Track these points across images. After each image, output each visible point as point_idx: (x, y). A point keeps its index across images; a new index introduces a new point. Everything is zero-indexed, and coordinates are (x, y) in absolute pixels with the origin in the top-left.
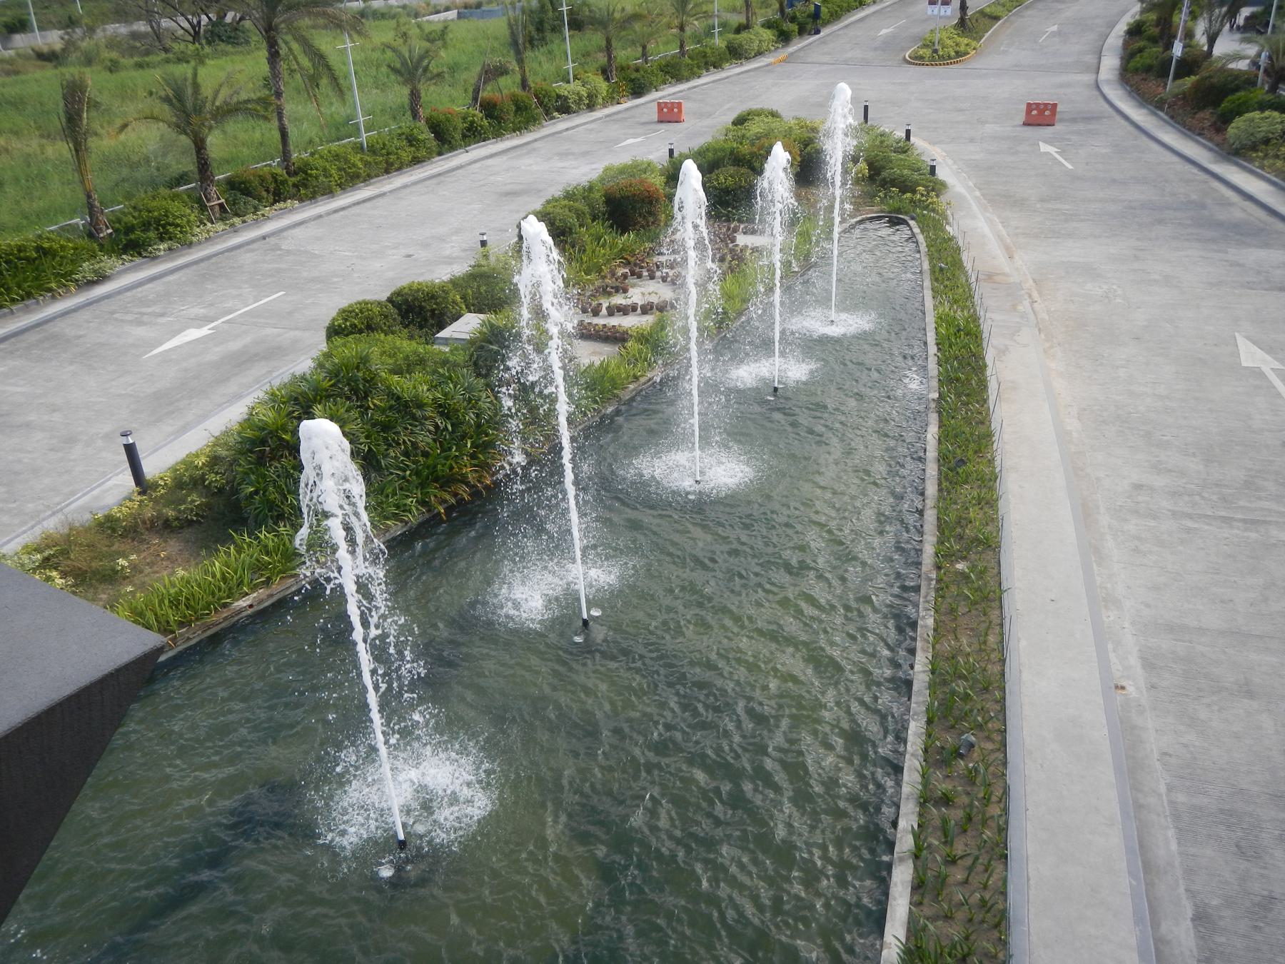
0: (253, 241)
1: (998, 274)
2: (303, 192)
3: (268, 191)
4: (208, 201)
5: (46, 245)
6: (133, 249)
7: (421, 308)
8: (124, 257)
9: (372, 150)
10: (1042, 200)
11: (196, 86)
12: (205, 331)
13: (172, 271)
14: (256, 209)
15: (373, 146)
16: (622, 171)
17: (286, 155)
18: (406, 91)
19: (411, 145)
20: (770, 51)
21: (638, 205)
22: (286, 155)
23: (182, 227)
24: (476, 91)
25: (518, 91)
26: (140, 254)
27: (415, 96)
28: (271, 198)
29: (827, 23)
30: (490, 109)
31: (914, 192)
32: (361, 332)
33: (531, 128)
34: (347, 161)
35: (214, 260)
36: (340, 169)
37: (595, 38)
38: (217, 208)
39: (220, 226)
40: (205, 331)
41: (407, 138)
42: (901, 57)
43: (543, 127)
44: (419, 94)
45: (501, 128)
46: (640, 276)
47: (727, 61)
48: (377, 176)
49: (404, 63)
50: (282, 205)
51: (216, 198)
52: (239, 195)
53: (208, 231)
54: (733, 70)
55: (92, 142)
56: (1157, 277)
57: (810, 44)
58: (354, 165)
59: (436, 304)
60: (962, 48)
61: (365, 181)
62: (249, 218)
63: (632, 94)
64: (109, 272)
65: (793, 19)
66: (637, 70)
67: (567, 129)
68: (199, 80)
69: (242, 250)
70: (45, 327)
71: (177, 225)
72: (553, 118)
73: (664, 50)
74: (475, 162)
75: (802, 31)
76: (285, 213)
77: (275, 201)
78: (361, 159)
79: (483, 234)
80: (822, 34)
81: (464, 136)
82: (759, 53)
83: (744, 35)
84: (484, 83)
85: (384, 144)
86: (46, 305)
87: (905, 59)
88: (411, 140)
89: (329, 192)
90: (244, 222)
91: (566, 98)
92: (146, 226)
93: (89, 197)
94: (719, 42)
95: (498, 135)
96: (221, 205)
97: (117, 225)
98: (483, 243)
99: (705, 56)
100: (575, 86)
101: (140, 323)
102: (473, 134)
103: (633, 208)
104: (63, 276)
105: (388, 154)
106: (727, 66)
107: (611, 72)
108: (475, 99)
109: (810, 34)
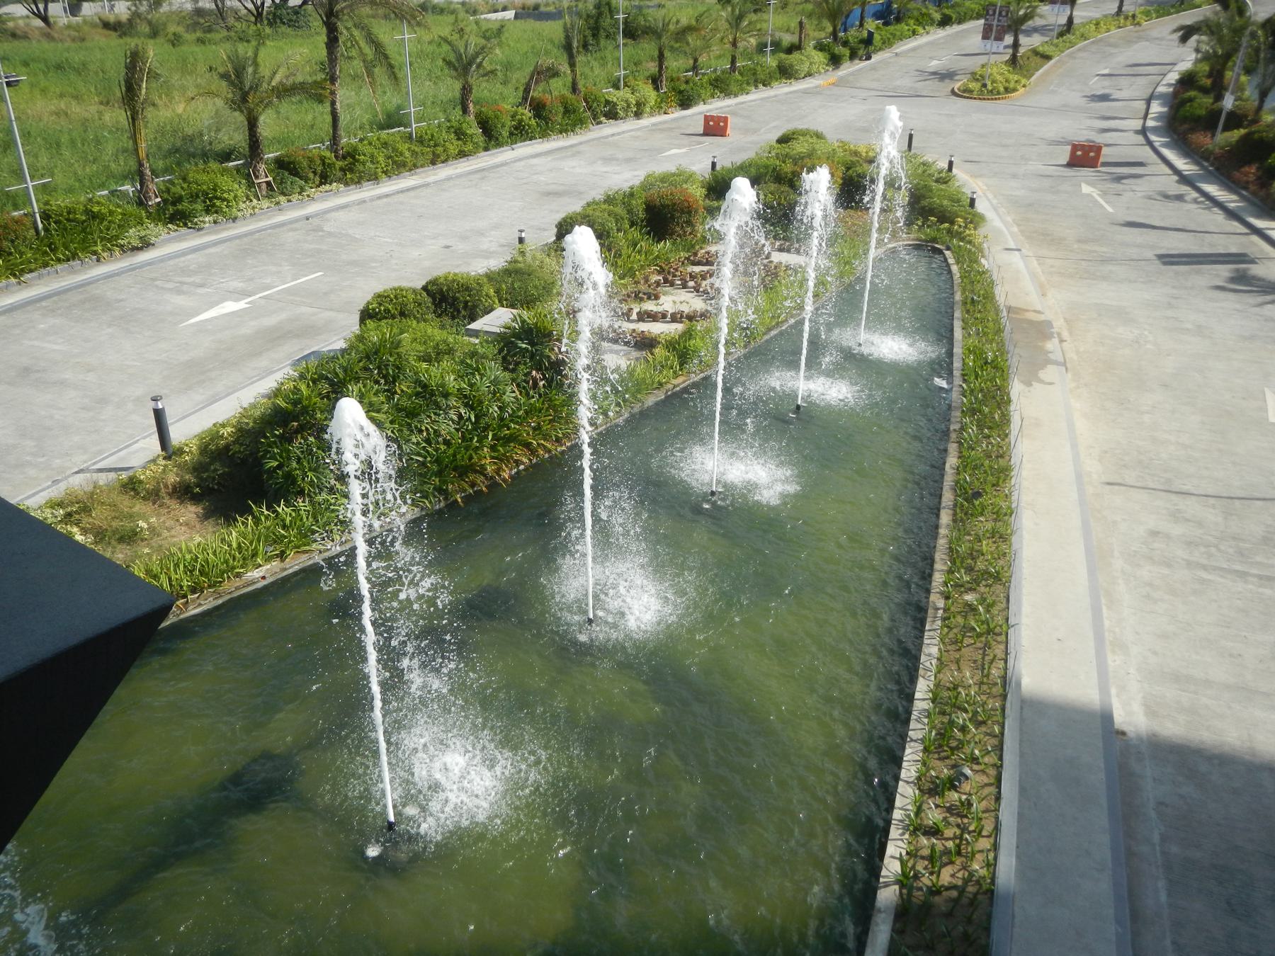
0: (297, 220)
1: (1027, 311)
2: (349, 176)
3: (315, 173)
4: (257, 177)
5: (96, 209)
6: (178, 220)
7: (455, 299)
8: (170, 226)
9: (421, 141)
10: (1079, 241)
11: (256, 64)
12: (242, 304)
13: (215, 244)
14: (302, 190)
15: (421, 137)
16: (664, 179)
17: (335, 139)
18: (458, 86)
19: (459, 139)
20: (820, 73)
21: (678, 215)
22: (335, 139)
23: (228, 202)
24: (527, 90)
25: (567, 93)
26: (185, 225)
27: (466, 90)
28: (317, 179)
30: (539, 109)
31: (952, 223)
32: (393, 317)
33: (577, 130)
34: (395, 150)
35: (257, 236)
37: (648, 47)
38: (264, 186)
39: (265, 203)
40: (242, 304)
41: (455, 132)
44: (471, 89)
46: (672, 285)
48: (422, 166)
49: (459, 57)
50: (327, 187)
51: (264, 176)
52: (286, 174)
53: (254, 208)
54: (782, 89)
55: (150, 113)
56: (1189, 326)
57: (860, 70)
58: (401, 154)
59: (469, 296)
60: (1012, 85)
61: (410, 170)
62: (295, 197)
63: (680, 106)
64: (153, 240)
65: (845, 44)
67: (613, 135)
68: (259, 60)
69: (285, 228)
70: (88, 288)
71: (224, 200)
72: (600, 123)
73: (715, 61)
74: (520, 160)
75: (853, 56)
76: (330, 196)
77: (321, 184)
78: (409, 149)
79: (521, 231)
80: (873, 60)
81: (511, 134)
82: (809, 75)
85: (432, 136)
86: (91, 267)
87: (953, 92)
88: (460, 134)
89: (374, 178)
90: (289, 201)
91: (615, 104)
92: (194, 197)
93: (141, 165)
95: (544, 135)
96: (268, 183)
97: (166, 196)
98: (521, 240)
99: (754, 74)
101: (179, 292)
102: (520, 133)
103: (673, 217)
104: (109, 240)
105: (436, 145)
106: (775, 84)
107: (661, 82)
108: (525, 99)
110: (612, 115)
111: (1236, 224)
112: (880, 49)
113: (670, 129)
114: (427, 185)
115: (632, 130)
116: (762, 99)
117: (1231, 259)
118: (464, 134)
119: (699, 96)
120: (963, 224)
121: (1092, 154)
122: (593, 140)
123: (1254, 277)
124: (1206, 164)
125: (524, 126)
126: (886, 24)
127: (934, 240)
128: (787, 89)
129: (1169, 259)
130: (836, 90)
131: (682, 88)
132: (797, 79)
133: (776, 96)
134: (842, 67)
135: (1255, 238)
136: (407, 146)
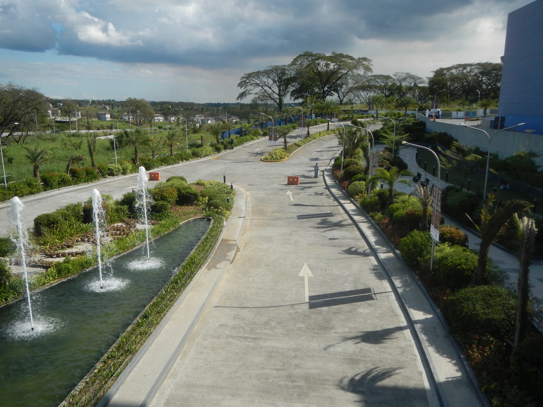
10: (272, 212)
19: (30, 187)
20: (211, 155)
24: (68, 166)
29: (236, 146)
30: (74, 173)
42: (260, 159)
43: (100, 181)
45: (78, 181)
46: (83, 241)
47: (192, 158)
54: (194, 162)
56: (292, 241)
57: (228, 153)
60: (283, 156)
65: (222, 144)
67: (110, 182)
72: (106, 177)
73: (166, 152)
74: (60, 194)
75: (225, 148)
80: (234, 149)
81: (59, 184)
82: (206, 155)
83: (200, 148)
84: (72, 163)
85: (15, 186)
87: (261, 159)
88: (30, 185)
91: (113, 170)
95: (76, 183)
99: (181, 156)
100: (118, 166)
102: (63, 183)
105: (16, 190)
110: (111, 174)
111: (336, 202)
112: (238, 145)
115: (120, 180)
116: (184, 165)
117: (325, 215)
118: (32, 185)
119: (154, 165)
120: (222, 209)
121: (296, 180)
122: (101, 184)
123: (328, 222)
124: (337, 181)
125: (65, 181)
126: (240, 136)
127: (209, 216)
128: (196, 161)
129: (300, 217)
130: (217, 161)
131: (146, 163)
132: (201, 157)
133: (190, 164)
134: (221, 152)
135: (340, 208)
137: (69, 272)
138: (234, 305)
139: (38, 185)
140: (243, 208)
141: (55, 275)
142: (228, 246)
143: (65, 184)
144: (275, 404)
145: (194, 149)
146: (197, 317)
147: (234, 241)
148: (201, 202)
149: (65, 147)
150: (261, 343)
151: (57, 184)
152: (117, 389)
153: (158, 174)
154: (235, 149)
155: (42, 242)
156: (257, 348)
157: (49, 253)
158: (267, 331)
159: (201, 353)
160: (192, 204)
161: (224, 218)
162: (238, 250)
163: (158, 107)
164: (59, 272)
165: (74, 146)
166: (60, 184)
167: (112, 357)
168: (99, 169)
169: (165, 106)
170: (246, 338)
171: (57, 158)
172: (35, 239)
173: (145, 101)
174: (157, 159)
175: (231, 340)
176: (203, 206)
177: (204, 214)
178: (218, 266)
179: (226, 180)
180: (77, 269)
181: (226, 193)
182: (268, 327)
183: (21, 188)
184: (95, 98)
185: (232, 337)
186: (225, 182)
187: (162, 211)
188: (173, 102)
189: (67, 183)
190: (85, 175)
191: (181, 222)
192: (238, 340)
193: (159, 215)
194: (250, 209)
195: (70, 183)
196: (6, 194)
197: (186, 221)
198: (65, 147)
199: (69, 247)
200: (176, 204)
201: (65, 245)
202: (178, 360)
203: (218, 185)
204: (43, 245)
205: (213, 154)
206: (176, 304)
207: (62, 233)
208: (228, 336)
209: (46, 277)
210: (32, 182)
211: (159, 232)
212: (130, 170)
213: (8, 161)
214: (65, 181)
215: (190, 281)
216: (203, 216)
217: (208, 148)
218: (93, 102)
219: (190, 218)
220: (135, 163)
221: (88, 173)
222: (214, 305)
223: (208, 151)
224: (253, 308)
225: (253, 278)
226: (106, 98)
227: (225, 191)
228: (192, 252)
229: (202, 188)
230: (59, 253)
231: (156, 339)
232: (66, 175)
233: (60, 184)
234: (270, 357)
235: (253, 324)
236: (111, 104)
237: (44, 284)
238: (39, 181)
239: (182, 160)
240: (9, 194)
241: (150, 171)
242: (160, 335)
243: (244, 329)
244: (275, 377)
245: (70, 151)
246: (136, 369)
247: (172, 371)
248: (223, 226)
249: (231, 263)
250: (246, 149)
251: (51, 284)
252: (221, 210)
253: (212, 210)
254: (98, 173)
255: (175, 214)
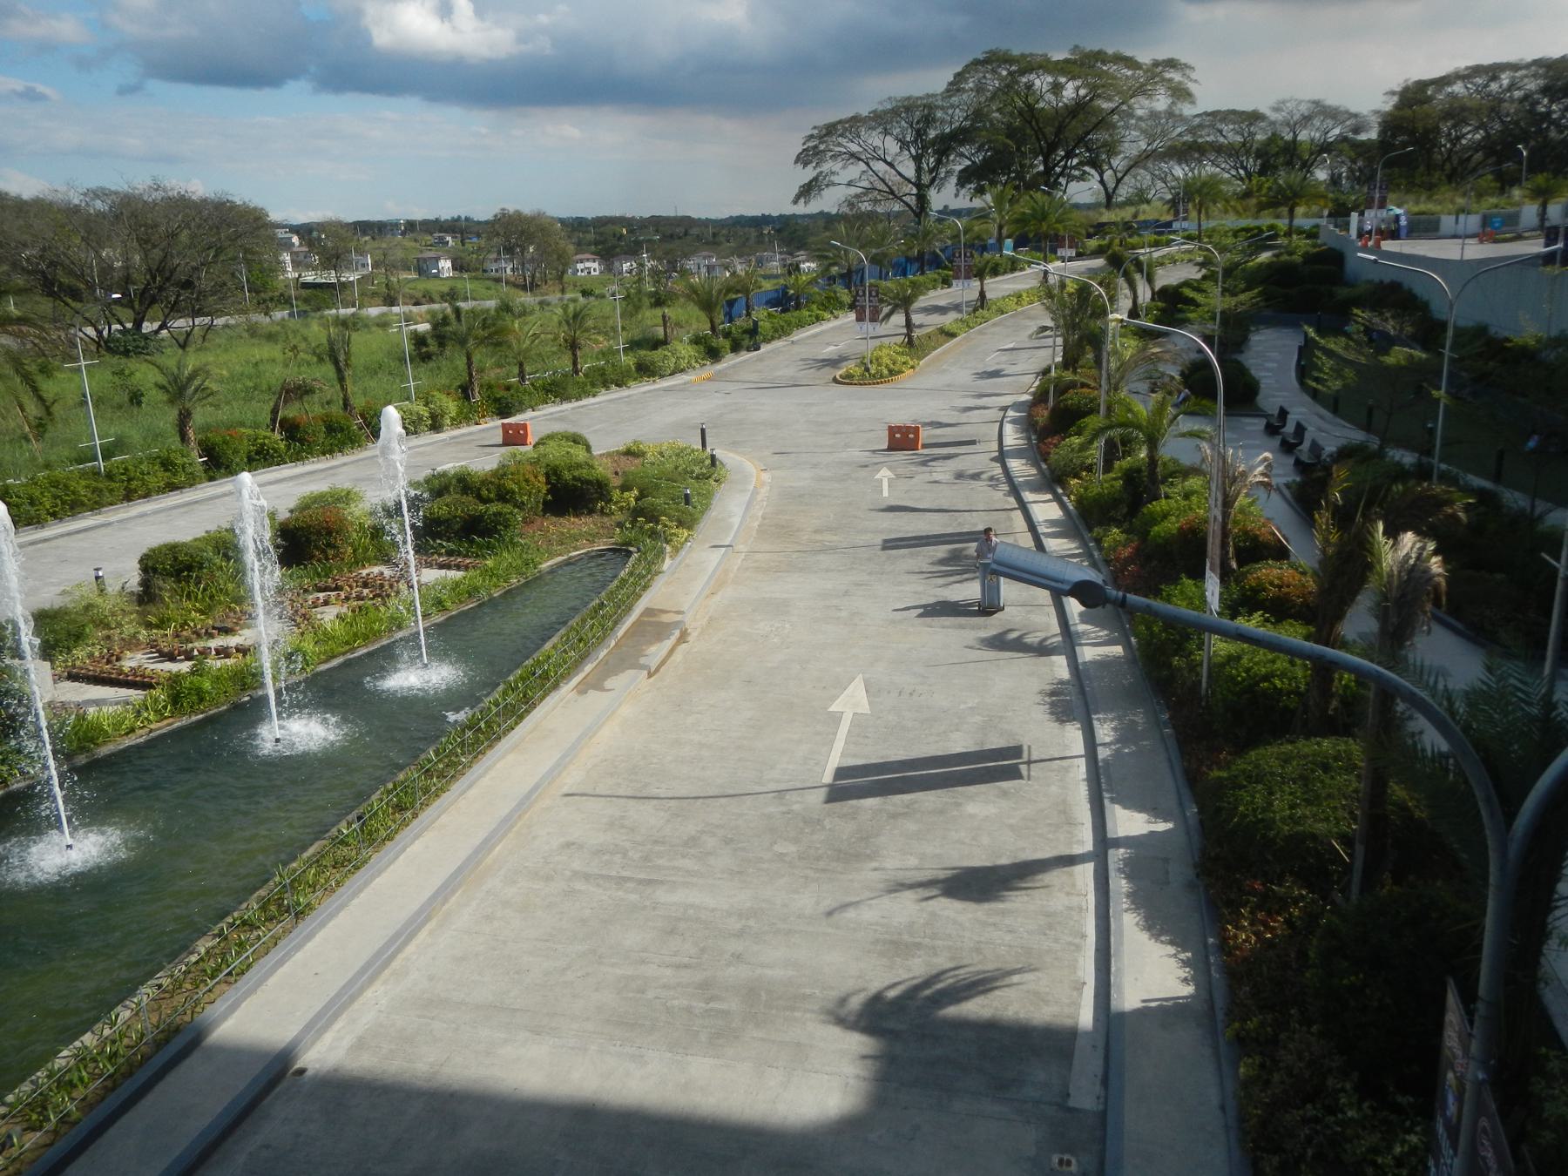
15: (110, 471)
19: (167, 470)
30: (291, 430)
36: (55, 497)
47: (635, 379)
57: (745, 361)
66: (508, 388)
75: (736, 348)
78: (87, 487)
85: (126, 469)
88: (167, 464)
94: (627, 360)
99: (603, 374)
105: (130, 480)
107: (473, 390)
108: (274, 421)
109: (748, 350)
112: (773, 338)
113: (469, 442)
114: (110, 524)
118: (173, 464)
119: (521, 403)
125: (268, 451)
131: (498, 396)
132: (662, 376)
136: (83, 483)
137: (201, 700)
138: (621, 792)
139: (190, 464)
140: (736, 521)
141: (165, 707)
142: (654, 627)
143: (265, 459)
144: (642, 1057)
145: (642, 353)
146: (507, 823)
147: (678, 612)
148: (616, 503)
149: (296, 356)
150: (661, 895)
151: (245, 460)
152: (234, 1008)
153: (524, 427)
154: (765, 348)
155: (154, 620)
156: (645, 907)
157: (166, 650)
158: (687, 861)
159: (489, 918)
160: (591, 512)
161: (668, 549)
162: (683, 638)
163: (590, 232)
164: (175, 699)
165: (314, 353)
166: (254, 460)
167: (248, 925)
168: (362, 416)
169: (610, 229)
170: (623, 880)
171: (264, 387)
172: (137, 612)
173: (547, 217)
174: (532, 384)
175: (579, 885)
176: (619, 517)
177: (618, 536)
178: (608, 684)
179: (708, 439)
180: (225, 692)
181: (697, 478)
182: (692, 851)
183: (144, 474)
184: (419, 214)
185: (587, 877)
186: (704, 445)
187: (497, 531)
188: (633, 218)
189: (272, 457)
190: (323, 435)
191: (546, 561)
192: (598, 885)
193: (489, 542)
194: (756, 524)
195: (280, 456)
196: (101, 491)
197: (560, 559)
198: (296, 356)
199: (227, 631)
200: (545, 511)
201: (214, 628)
202: (423, 935)
203: (678, 455)
204: (158, 627)
205: (698, 366)
206: (456, 787)
207: (212, 597)
208: (575, 874)
209: (139, 712)
210: (172, 456)
211: (476, 589)
212: (453, 419)
213: (131, 400)
214: (268, 453)
215: (517, 723)
216: (613, 544)
217: (684, 349)
218: (411, 226)
219: (576, 549)
220: (467, 398)
221: (332, 428)
222: (565, 790)
223: (684, 358)
224: (671, 798)
225: (699, 716)
226: (446, 215)
227: (692, 472)
228: (548, 646)
229: (632, 466)
230: (192, 650)
231: (377, 880)
232: (268, 434)
233: (254, 460)
234: (672, 932)
235: (656, 842)
236: (460, 228)
237: (132, 730)
238: (195, 454)
239: (606, 385)
240: (111, 491)
241: (506, 421)
242: (389, 870)
243: (625, 855)
244: (665, 986)
245: (302, 369)
246: (299, 956)
247: (395, 964)
248: (658, 573)
249: (650, 675)
250: (796, 348)
251: (151, 731)
252: (666, 526)
253: (641, 528)
254: (360, 429)
255: (536, 539)
